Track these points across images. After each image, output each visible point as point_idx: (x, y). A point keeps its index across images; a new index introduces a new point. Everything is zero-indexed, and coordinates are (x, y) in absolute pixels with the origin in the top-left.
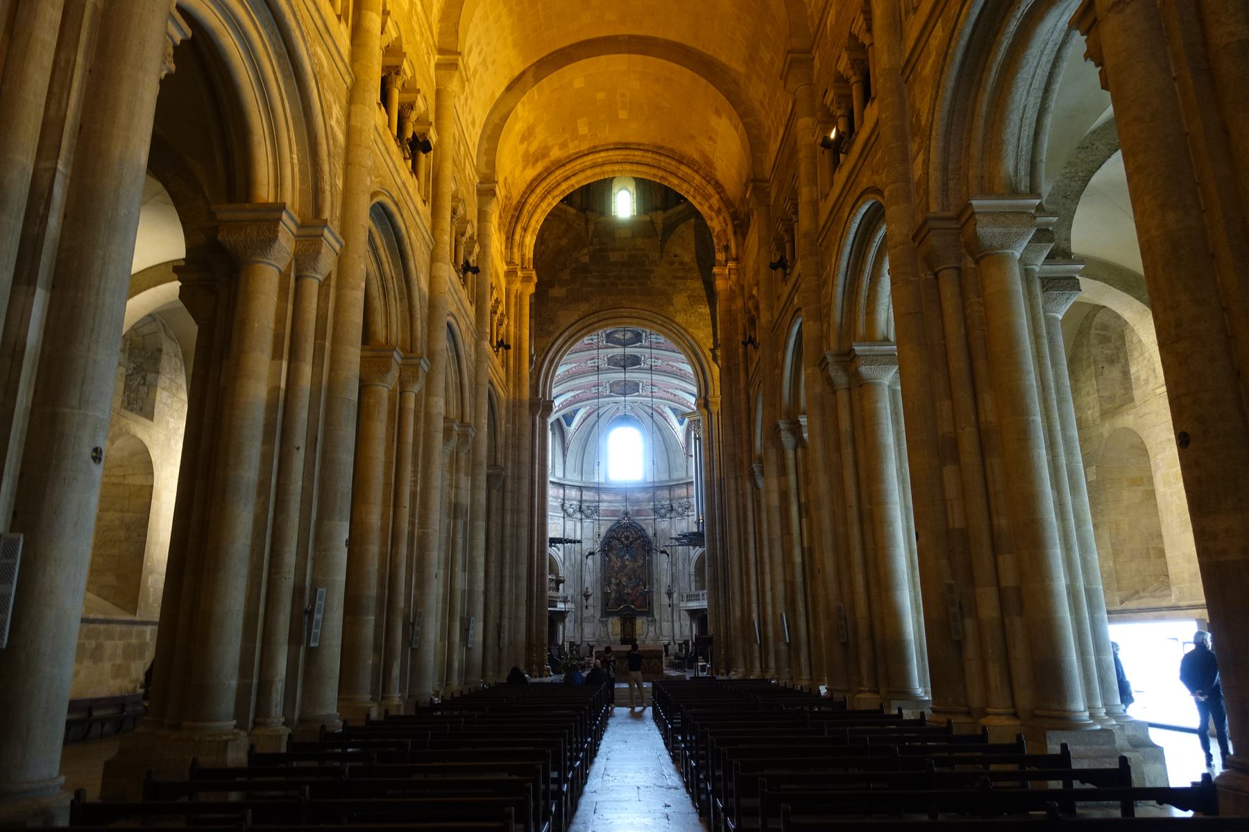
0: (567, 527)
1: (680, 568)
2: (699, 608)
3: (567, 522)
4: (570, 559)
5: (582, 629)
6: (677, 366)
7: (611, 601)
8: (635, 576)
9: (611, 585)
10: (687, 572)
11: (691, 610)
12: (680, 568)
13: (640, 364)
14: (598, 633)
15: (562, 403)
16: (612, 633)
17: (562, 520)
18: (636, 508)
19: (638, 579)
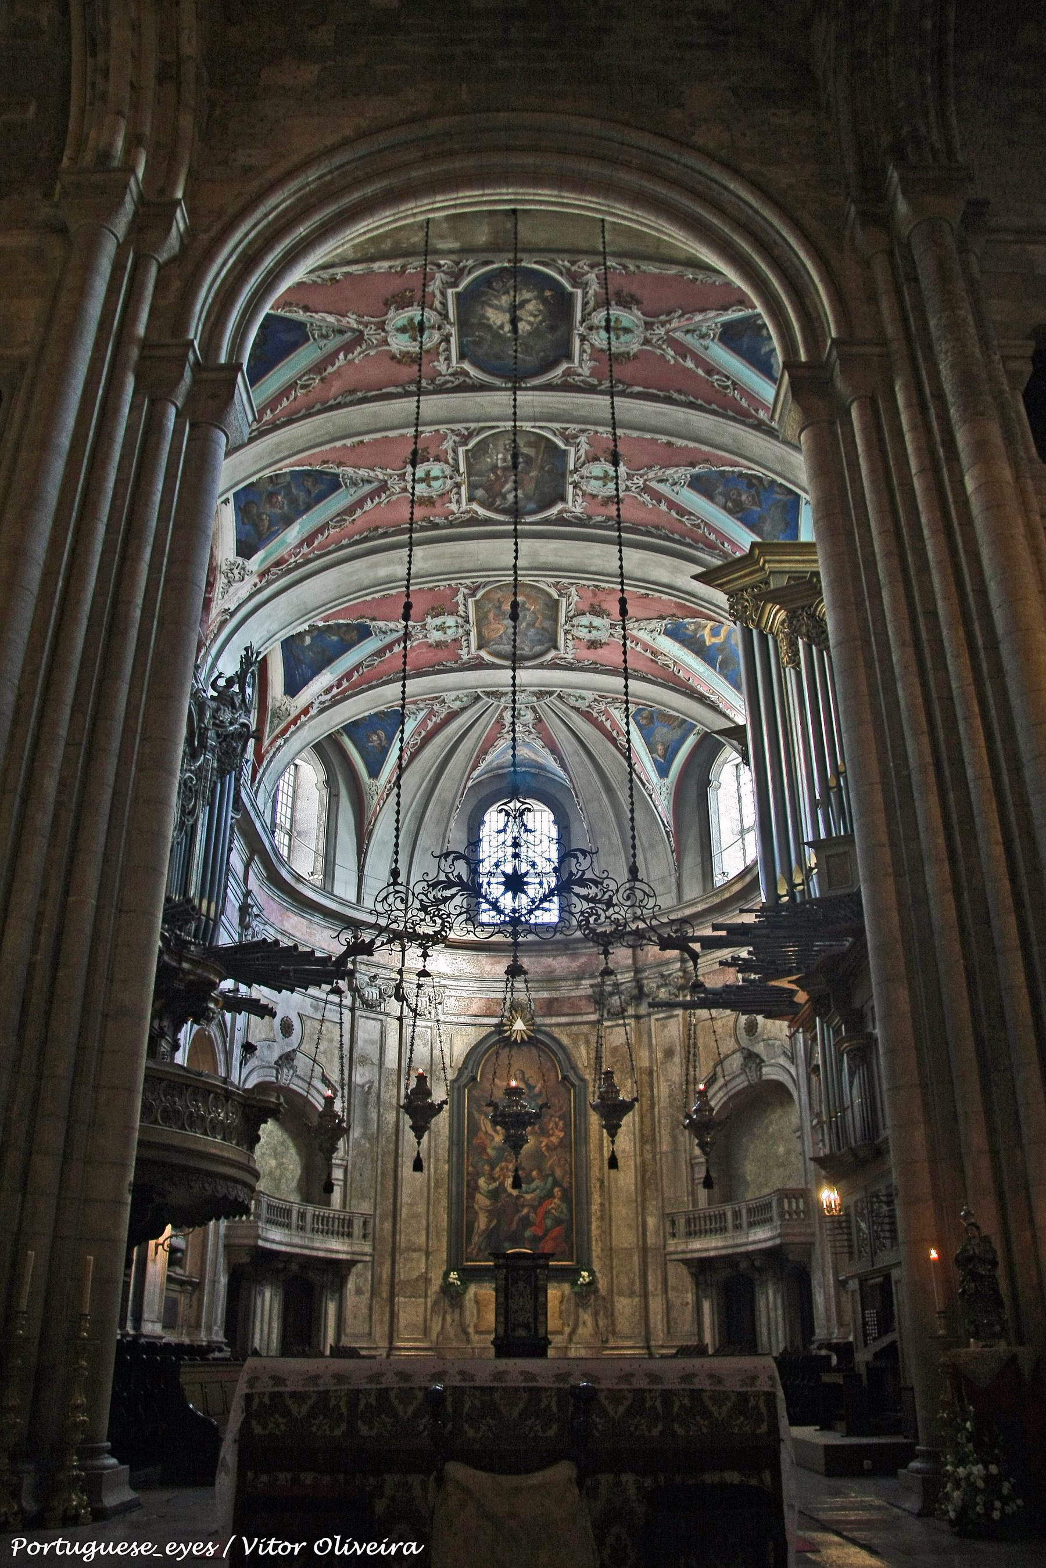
0: (361, 1035)
1: (665, 1148)
2: (723, 1252)
3: (361, 1023)
4: (366, 1122)
5: (393, 1316)
6: (672, 496)
7: (476, 1239)
8: (540, 1171)
9: (478, 1196)
10: (683, 1157)
11: (702, 1261)
12: (665, 1148)
13: (563, 498)
14: (436, 1327)
15: (348, 675)
16: (476, 1326)
17: (347, 1014)
18: (545, 995)
19: (550, 1180)
